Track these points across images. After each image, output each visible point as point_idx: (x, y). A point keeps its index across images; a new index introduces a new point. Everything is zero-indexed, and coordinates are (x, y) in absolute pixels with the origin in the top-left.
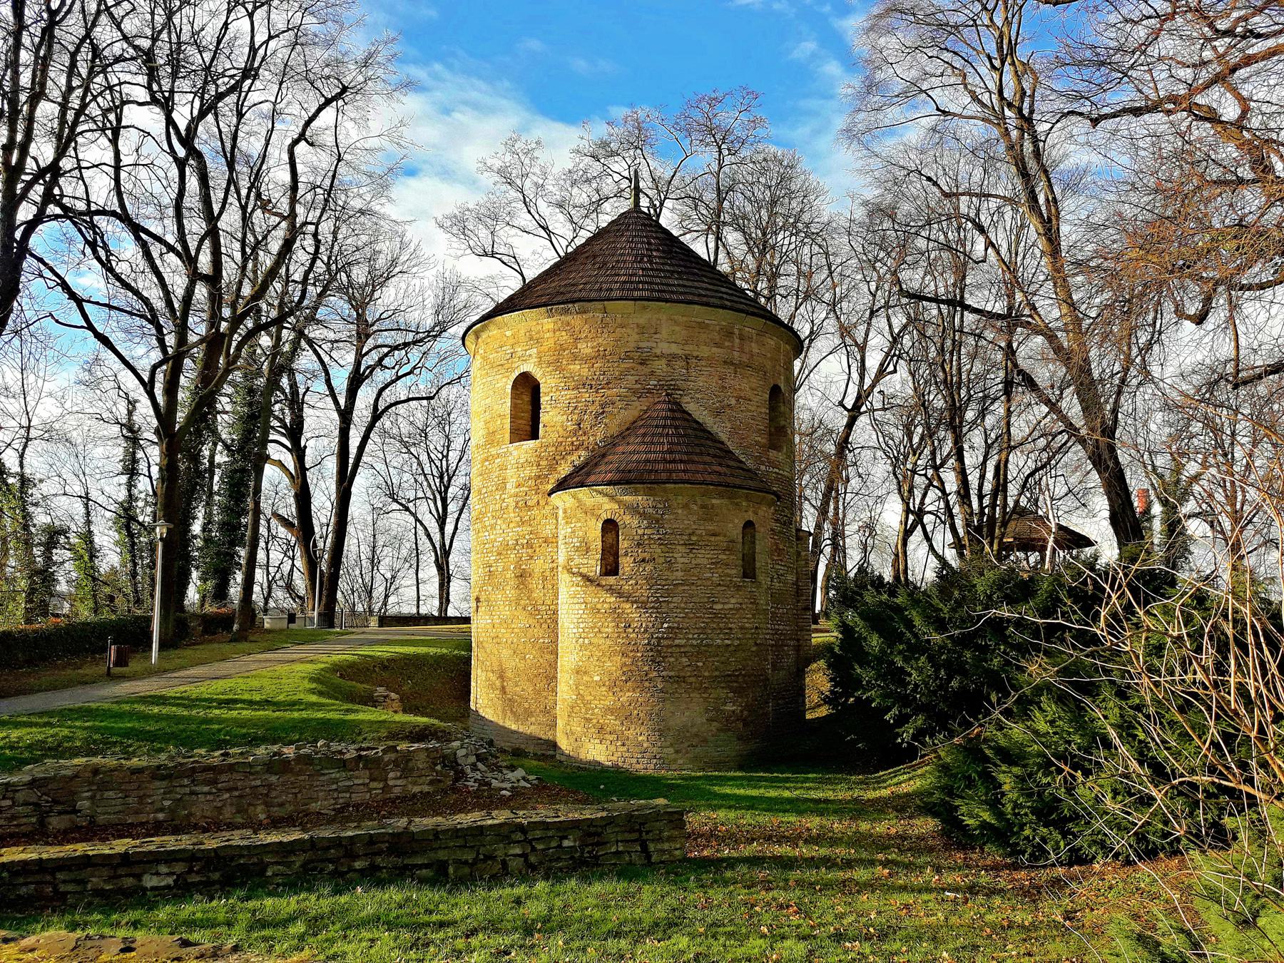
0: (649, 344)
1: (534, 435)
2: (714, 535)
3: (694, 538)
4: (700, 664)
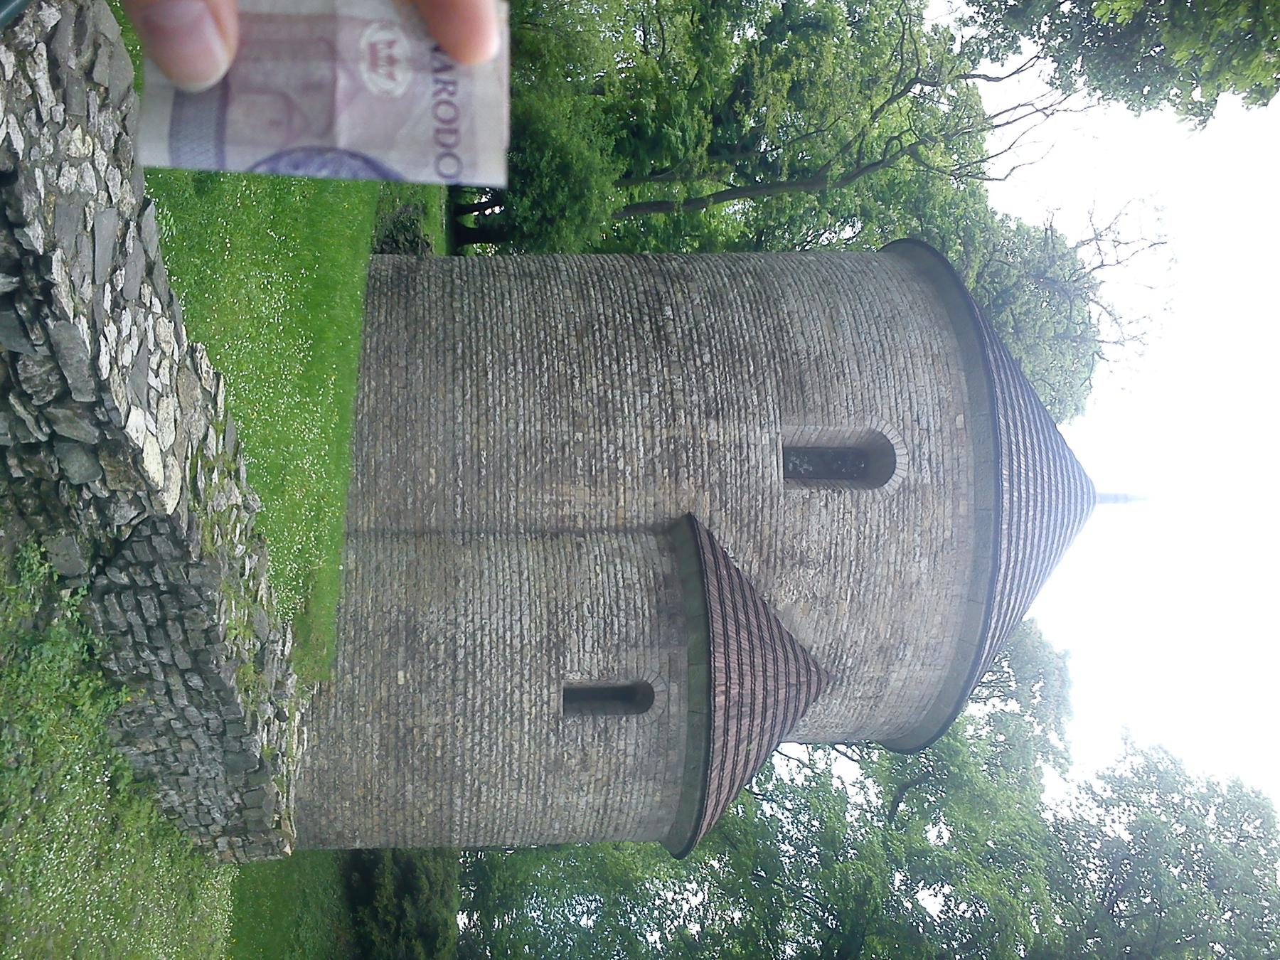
0: (908, 657)
1: (792, 475)
2: (616, 829)
3: (615, 814)
4: (423, 824)
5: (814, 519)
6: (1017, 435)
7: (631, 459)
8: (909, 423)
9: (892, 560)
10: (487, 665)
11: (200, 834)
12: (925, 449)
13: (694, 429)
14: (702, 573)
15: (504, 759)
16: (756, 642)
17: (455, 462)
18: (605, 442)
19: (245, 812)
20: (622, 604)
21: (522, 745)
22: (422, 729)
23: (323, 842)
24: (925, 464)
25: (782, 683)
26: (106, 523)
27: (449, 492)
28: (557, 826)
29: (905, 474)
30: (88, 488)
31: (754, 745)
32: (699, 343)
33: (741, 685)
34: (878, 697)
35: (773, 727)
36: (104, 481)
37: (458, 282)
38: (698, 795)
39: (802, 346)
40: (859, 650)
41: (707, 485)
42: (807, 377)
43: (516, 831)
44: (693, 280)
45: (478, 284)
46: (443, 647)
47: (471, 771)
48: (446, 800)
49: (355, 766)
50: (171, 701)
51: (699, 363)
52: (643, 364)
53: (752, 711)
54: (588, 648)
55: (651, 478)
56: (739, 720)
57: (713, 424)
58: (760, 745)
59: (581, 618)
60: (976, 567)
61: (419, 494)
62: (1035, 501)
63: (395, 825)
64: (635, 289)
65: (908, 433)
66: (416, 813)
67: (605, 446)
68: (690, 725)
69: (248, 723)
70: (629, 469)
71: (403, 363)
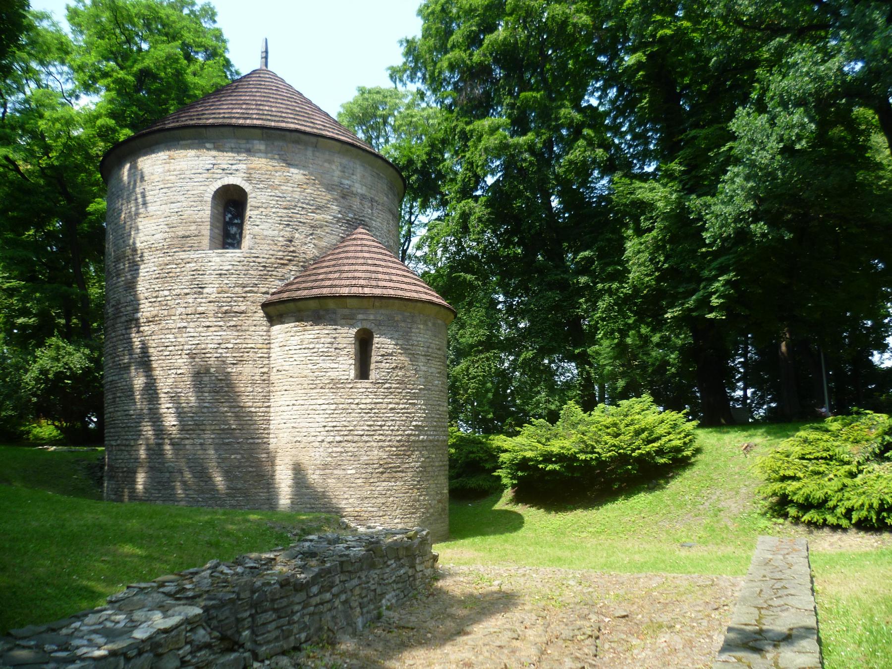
2: (439, 349)
3: (430, 350)
5: (265, 233)
6: (220, 113)
7: (227, 339)
8: (210, 175)
9: (291, 189)
10: (345, 424)
11: (415, 580)
12: (225, 166)
13: (210, 302)
14: (294, 300)
15: (398, 413)
16: (337, 268)
17: (228, 444)
18: (216, 355)
19: (401, 556)
20: (311, 346)
21: (390, 403)
22: (380, 459)
23: (443, 510)
24: (234, 167)
25: (360, 255)
26: (208, 646)
27: (246, 447)
28: (437, 382)
29: (240, 179)
30: (184, 657)
31: (394, 271)
32: (156, 297)
33: (359, 278)
34: (372, 200)
35: (385, 261)
36: (179, 649)
37: (119, 442)
38: (419, 304)
39: (159, 236)
40: (344, 210)
41: (244, 295)
42: (180, 234)
43: (439, 405)
44: (119, 300)
45: (120, 429)
46: (335, 449)
47: (404, 431)
48: (420, 444)
49: (401, 495)
50: (328, 602)
51: (169, 298)
52: (169, 331)
53: (375, 272)
54: (336, 366)
55: (239, 328)
56: (379, 280)
57: (205, 291)
58: (394, 268)
59: (320, 370)
60: (297, 142)
61: (247, 464)
62: (260, 105)
63: (434, 472)
64: (123, 335)
65: (215, 176)
66: (428, 460)
67: (218, 355)
68: (381, 307)
69: (344, 559)
70: (232, 341)
71: (167, 475)
